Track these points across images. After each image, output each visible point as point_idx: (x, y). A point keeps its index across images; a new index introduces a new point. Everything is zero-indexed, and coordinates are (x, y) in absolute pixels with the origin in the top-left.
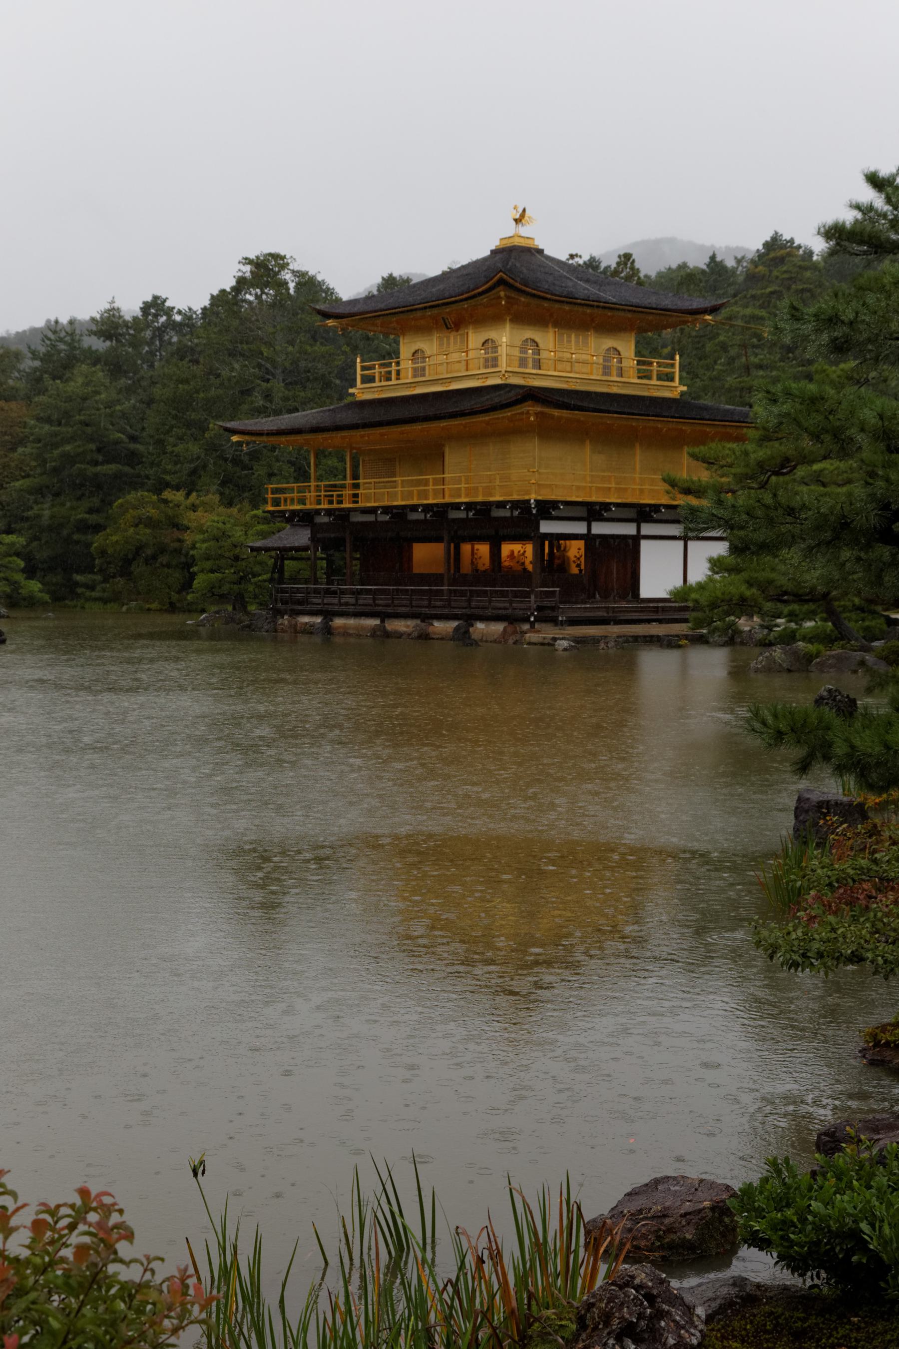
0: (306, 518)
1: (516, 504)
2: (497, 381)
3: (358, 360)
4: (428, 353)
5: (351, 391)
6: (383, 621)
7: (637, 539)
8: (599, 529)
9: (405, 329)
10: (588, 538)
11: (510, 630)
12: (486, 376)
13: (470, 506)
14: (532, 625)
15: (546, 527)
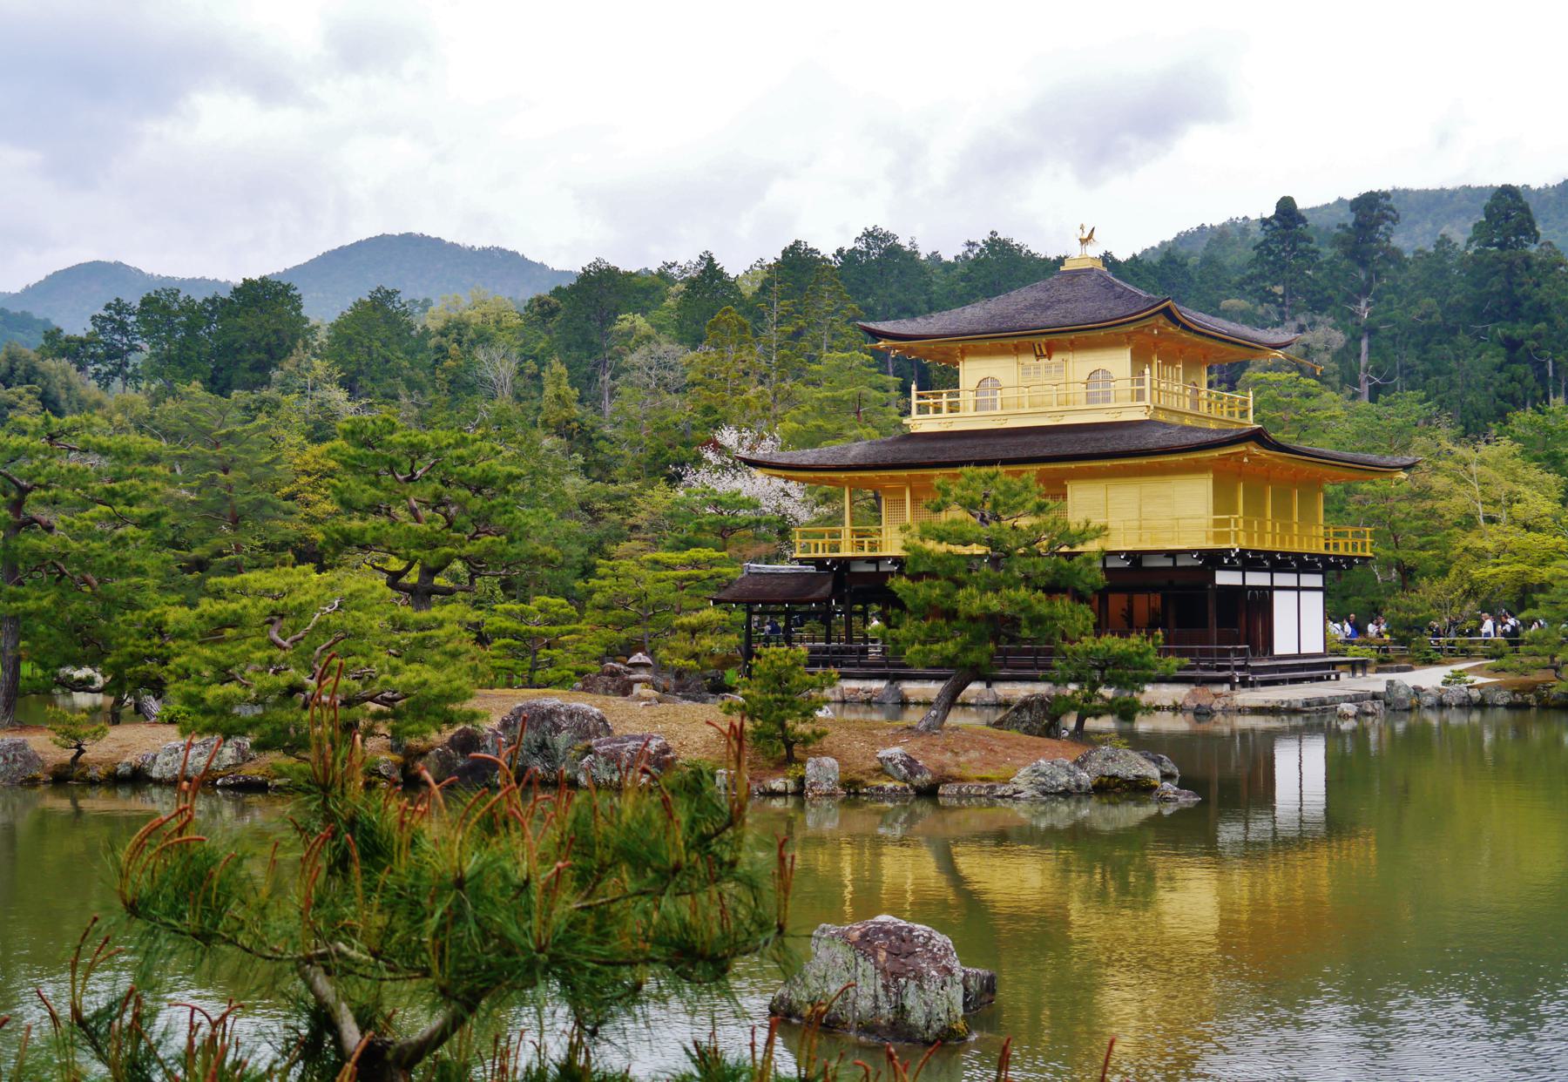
0: (845, 563)
1: (1203, 553)
2: (1142, 417)
3: (914, 387)
4: (1003, 383)
5: (906, 421)
6: (989, 686)
7: (1272, 588)
8: (1257, 579)
9: (964, 353)
10: (1243, 589)
11: (1199, 690)
12: (1120, 410)
13: (1130, 555)
14: (1232, 688)
15: (1224, 578)
